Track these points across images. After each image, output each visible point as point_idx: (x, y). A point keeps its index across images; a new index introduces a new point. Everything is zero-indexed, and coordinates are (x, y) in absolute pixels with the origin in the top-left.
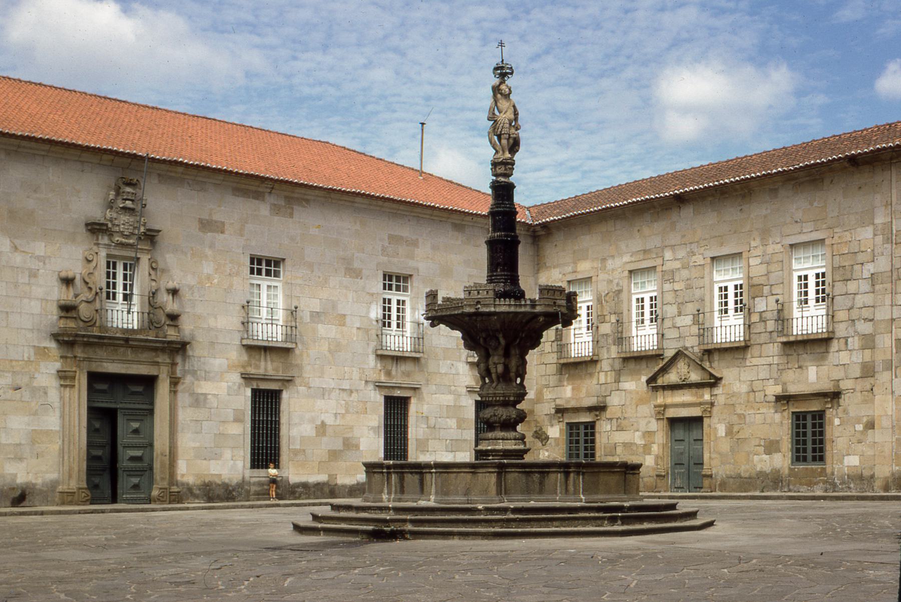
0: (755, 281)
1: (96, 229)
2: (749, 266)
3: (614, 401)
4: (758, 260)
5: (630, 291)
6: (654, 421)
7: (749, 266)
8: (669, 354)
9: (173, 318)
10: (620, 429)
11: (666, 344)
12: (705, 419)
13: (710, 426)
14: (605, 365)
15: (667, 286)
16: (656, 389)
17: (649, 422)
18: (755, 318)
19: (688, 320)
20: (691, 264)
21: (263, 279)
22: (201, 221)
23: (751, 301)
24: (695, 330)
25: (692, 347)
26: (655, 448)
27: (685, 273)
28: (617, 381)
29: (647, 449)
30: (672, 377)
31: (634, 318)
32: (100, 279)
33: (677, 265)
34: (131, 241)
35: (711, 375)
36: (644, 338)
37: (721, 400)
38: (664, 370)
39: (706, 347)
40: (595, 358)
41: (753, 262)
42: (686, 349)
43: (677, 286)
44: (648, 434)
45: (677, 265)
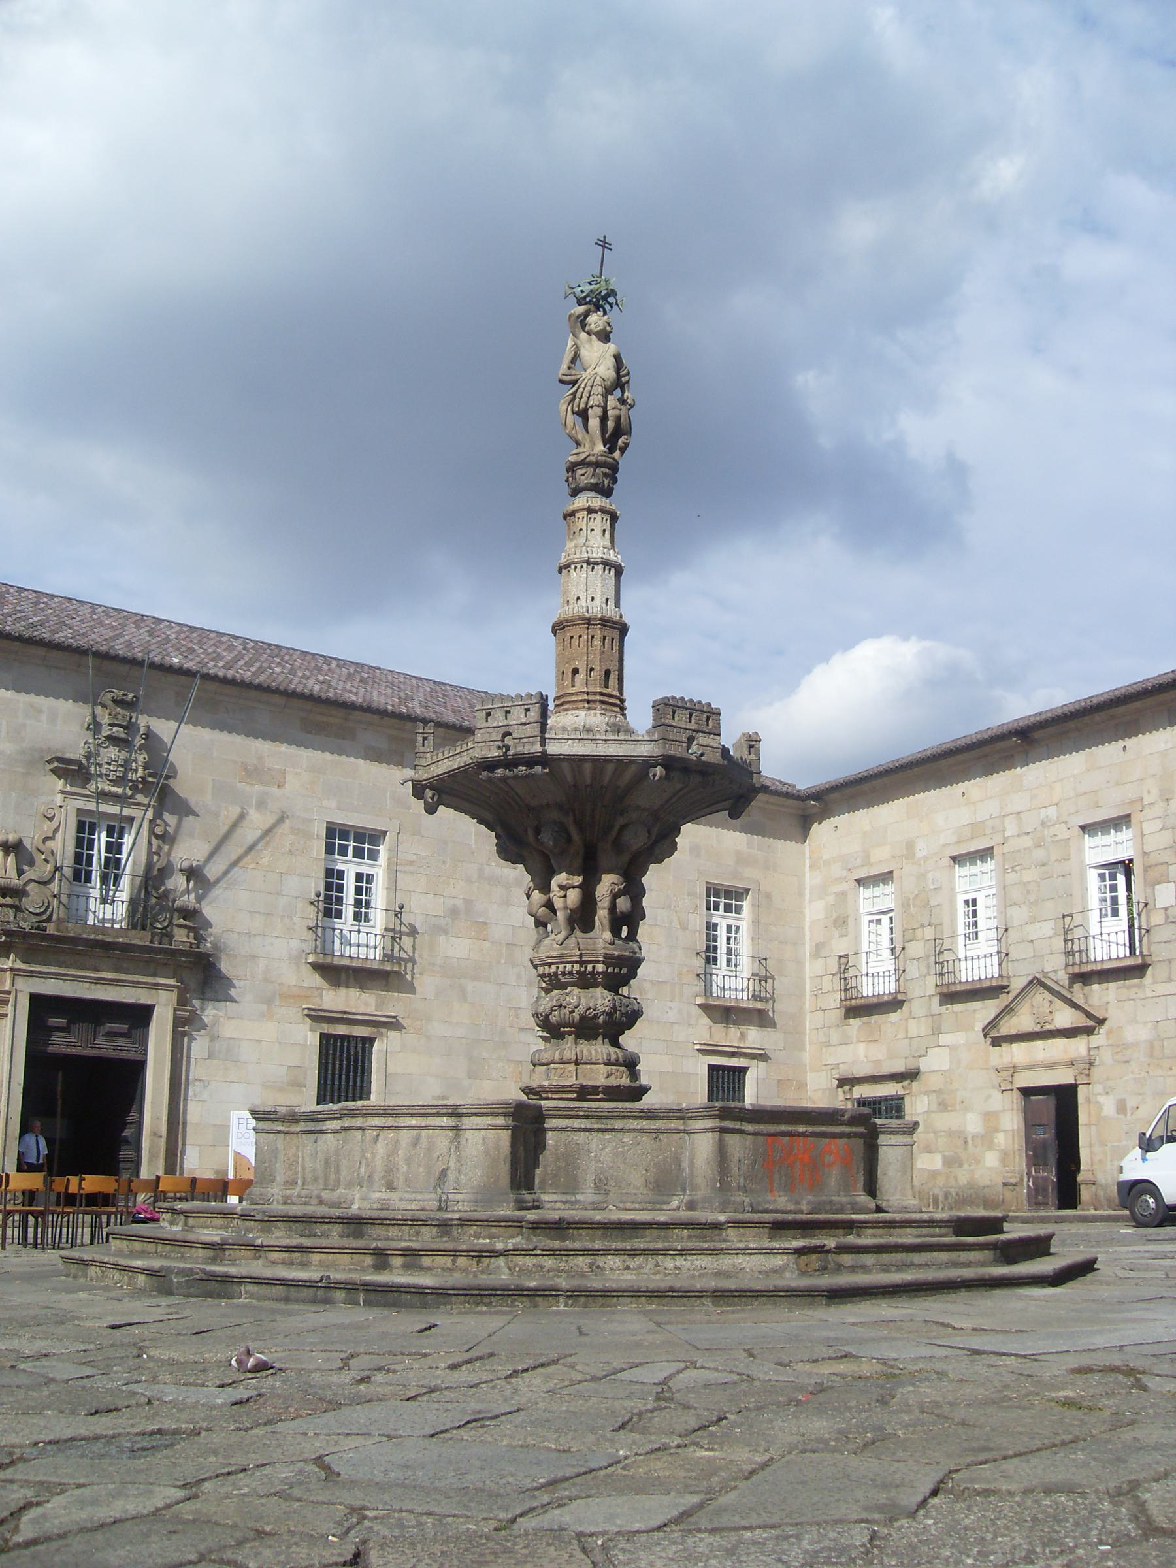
0: (1154, 858)
1: (73, 771)
2: (1143, 835)
3: (934, 1062)
4: (1158, 824)
5: (953, 889)
6: (997, 1094)
7: (1143, 835)
8: (1017, 984)
9: (189, 914)
10: (943, 1106)
11: (1011, 968)
12: (1080, 1089)
13: (1088, 1101)
14: (916, 1007)
15: (1011, 877)
16: (997, 1042)
17: (989, 1096)
18: (1157, 918)
19: (1047, 928)
20: (1049, 839)
21: (350, 862)
22: (244, 767)
23: (1149, 890)
24: (1059, 944)
25: (1055, 971)
26: (1000, 1139)
27: (1040, 854)
28: (937, 1032)
29: (986, 1139)
30: (1022, 1021)
31: (961, 929)
32: (64, 846)
33: (1027, 842)
34: (120, 790)
35: (1088, 1015)
36: (977, 962)
37: (1105, 1057)
38: (1007, 1010)
39: (1077, 970)
40: (900, 997)
41: (1148, 827)
42: (1045, 974)
43: (1029, 876)
44: (990, 1117)
45: (1027, 842)
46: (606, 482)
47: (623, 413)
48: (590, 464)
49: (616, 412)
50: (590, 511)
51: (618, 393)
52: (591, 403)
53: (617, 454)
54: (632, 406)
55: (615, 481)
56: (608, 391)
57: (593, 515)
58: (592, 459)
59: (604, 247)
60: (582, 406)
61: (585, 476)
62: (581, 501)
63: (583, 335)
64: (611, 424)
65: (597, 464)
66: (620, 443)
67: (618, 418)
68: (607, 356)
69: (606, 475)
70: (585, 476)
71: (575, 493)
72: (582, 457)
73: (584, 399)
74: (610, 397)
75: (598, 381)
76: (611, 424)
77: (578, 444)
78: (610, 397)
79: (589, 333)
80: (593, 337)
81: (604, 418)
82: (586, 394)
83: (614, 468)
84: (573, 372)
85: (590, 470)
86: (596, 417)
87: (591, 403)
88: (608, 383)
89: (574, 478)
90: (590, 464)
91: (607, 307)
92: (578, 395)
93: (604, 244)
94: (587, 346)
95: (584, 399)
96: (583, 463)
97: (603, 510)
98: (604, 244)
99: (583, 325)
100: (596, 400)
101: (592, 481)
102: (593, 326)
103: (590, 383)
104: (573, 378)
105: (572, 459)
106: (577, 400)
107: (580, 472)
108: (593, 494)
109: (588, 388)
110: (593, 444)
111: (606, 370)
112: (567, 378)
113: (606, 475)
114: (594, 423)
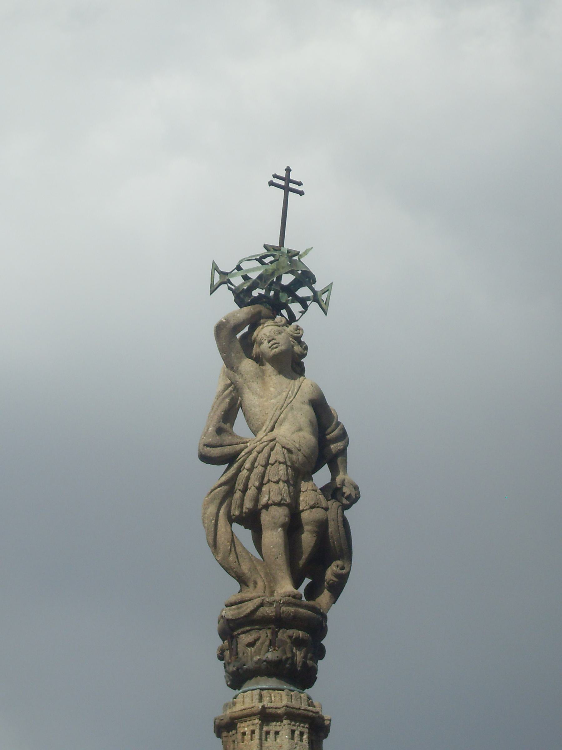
46: (299, 656)
47: (331, 515)
48: (264, 622)
49: (317, 514)
50: (267, 716)
51: (322, 477)
52: (264, 500)
53: (324, 597)
54: (353, 500)
55: (320, 653)
56: (301, 473)
57: (273, 727)
58: (268, 611)
59: (287, 190)
60: (248, 504)
61: (257, 648)
62: (248, 699)
63: (247, 365)
64: (308, 539)
65: (279, 622)
66: (330, 574)
67: (322, 527)
68: (296, 403)
69: (298, 643)
70: (257, 648)
71: (237, 680)
72: (248, 607)
73: (251, 492)
74: (304, 486)
75: (278, 454)
76: (308, 539)
77: (242, 580)
78: (304, 486)
79: (259, 360)
80: (269, 368)
81: (293, 528)
82: (254, 482)
83: (316, 628)
84: (227, 439)
85: (265, 634)
86: (275, 526)
87: (264, 500)
88: (298, 457)
89: (235, 653)
90: (264, 622)
91: (296, 308)
92: (239, 486)
93: (287, 184)
94: (255, 386)
95: (251, 492)
96: (250, 621)
97: (293, 715)
98: (287, 184)
99: (248, 344)
100: (274, 492)
101: (270, 656)
102: (265, 346)
103: (261, 459)
104: (227, 450)
105: (230, 613)
106: (238, 494)
107: (245, 639)
108: (273, 682)
109: (259, 470)
110: (272, 581)
111: (294, 431)
112: (215, 452)
113: (298, 643)
114: (273, 538)
